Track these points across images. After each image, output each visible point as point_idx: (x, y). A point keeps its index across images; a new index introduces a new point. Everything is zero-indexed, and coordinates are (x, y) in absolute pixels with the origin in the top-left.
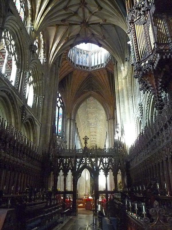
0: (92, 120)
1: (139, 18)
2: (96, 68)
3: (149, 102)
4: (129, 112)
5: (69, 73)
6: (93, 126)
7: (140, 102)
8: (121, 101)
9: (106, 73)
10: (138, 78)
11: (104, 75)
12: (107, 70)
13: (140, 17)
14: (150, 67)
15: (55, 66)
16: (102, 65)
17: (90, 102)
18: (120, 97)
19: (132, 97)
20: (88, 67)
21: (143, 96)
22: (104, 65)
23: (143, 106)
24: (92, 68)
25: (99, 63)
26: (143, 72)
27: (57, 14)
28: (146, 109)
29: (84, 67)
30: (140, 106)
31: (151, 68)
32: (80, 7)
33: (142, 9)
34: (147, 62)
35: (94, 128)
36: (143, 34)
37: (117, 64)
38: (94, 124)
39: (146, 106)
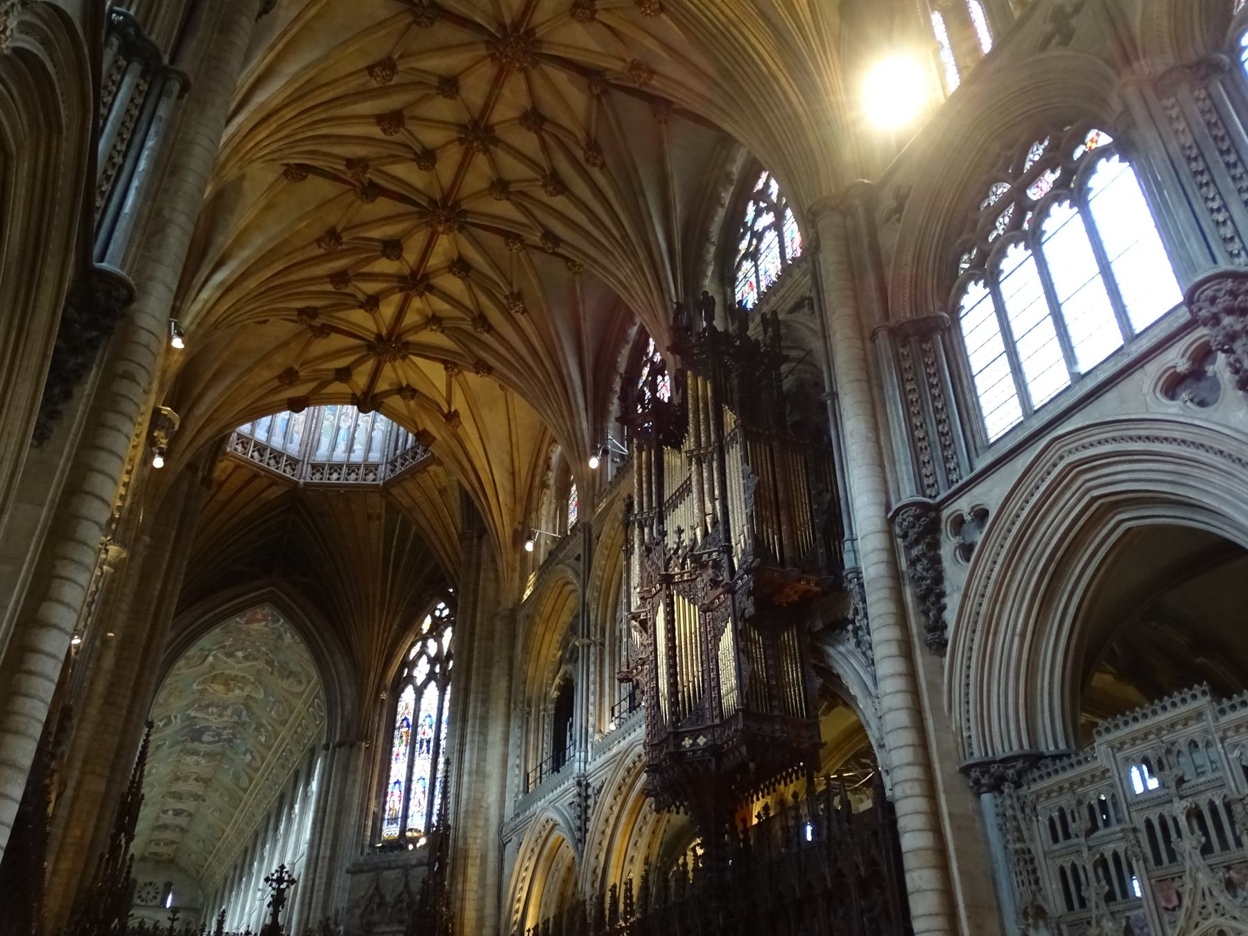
0: (212, 714)
2: (335, 476)
3: (624, 789)
4: (504, 778)
6: (203, 748)
7: (582, 771)
8: (475, 714)
13: (694, 577)
14: (710, 761)
16: (371, 468)
17: (245, 627)
18: (472, 697)
20: (297, 462)
23: (590, 791)
24: (317, 467)
25: (357, 456)
29: (277, 455)
32: (401, 290)
34: (701, 741)
35: (206, 755)
36: (696, 636)
37: (480, 538)
38: (219, 735)
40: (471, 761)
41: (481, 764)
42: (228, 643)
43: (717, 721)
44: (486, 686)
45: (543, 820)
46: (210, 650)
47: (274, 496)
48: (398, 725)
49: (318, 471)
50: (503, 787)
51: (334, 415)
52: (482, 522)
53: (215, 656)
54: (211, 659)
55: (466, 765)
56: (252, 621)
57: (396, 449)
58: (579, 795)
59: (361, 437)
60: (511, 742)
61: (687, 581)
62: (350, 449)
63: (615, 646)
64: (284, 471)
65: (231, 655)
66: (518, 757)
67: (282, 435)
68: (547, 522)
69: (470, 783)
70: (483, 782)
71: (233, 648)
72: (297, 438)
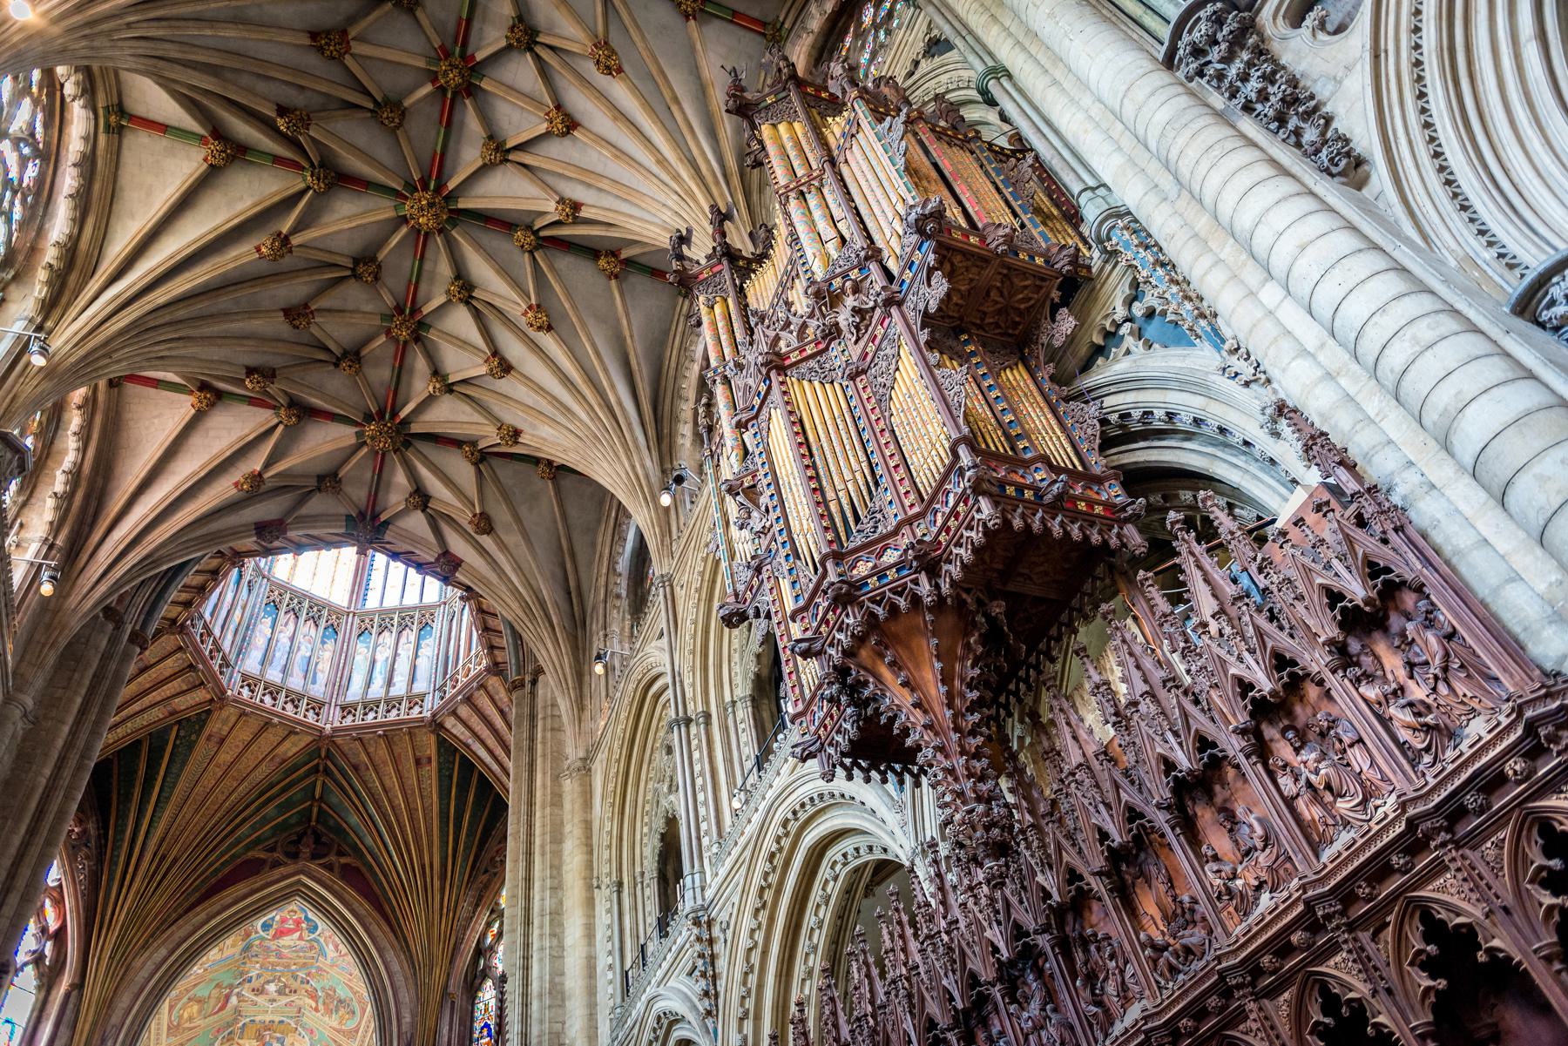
1: (820, 353)
2: (371, 715)
3: (769, 896)
4: (591, 991)
5: (179, 722)
7: (699, 902)
9: (432, 751)
10: (819, 654)
11: (418, 762)
12: (438, 735)
13: (822, 346)
14: (916, 582)
15: (110, 626)
16: (415, 700)
18: (537, 885)
19: (620, 884)
20: (321, 705)
21: (729, 862)
22: (428, 704)
24: (347, 709)
25: (399, 689)
26: (873, 615)
27: (236, 326)
28: (744, 942)
29: (295, 699)
30: (696, 931)
31: (925, 588)
33: (850, 301)
34: (891, 557)
37: (534, 682)
39: (747, 922)
40: (541, 978)
41: (557, 980)
42: (253, 974)
43: (916, 509)
44: (556, 868)
45: (651, 1022)
46: (231, 987)
47: (294, 750)
48: (476, 1036)
49: (350, 712)
50: (592, 1006)
51: (368, 648)
52: (536, 660)
53: (238, 995)
54: (234, 1000)
55: (535, 987)
56: (281, 933)
57: (445, 673)
58: (699, 939)
59: (403, 667)
60: (599, 936)
61: (812, 356)
62: (389, 683)
63: (726, 719)
64: (305, 716)
65: (259, 991)
66: (610, 953)
67: (301, 675)
68: (620, 642)
69: (542, 1008)
70: (562, 1006)
71: (262, 980)
72: (322, 678)
